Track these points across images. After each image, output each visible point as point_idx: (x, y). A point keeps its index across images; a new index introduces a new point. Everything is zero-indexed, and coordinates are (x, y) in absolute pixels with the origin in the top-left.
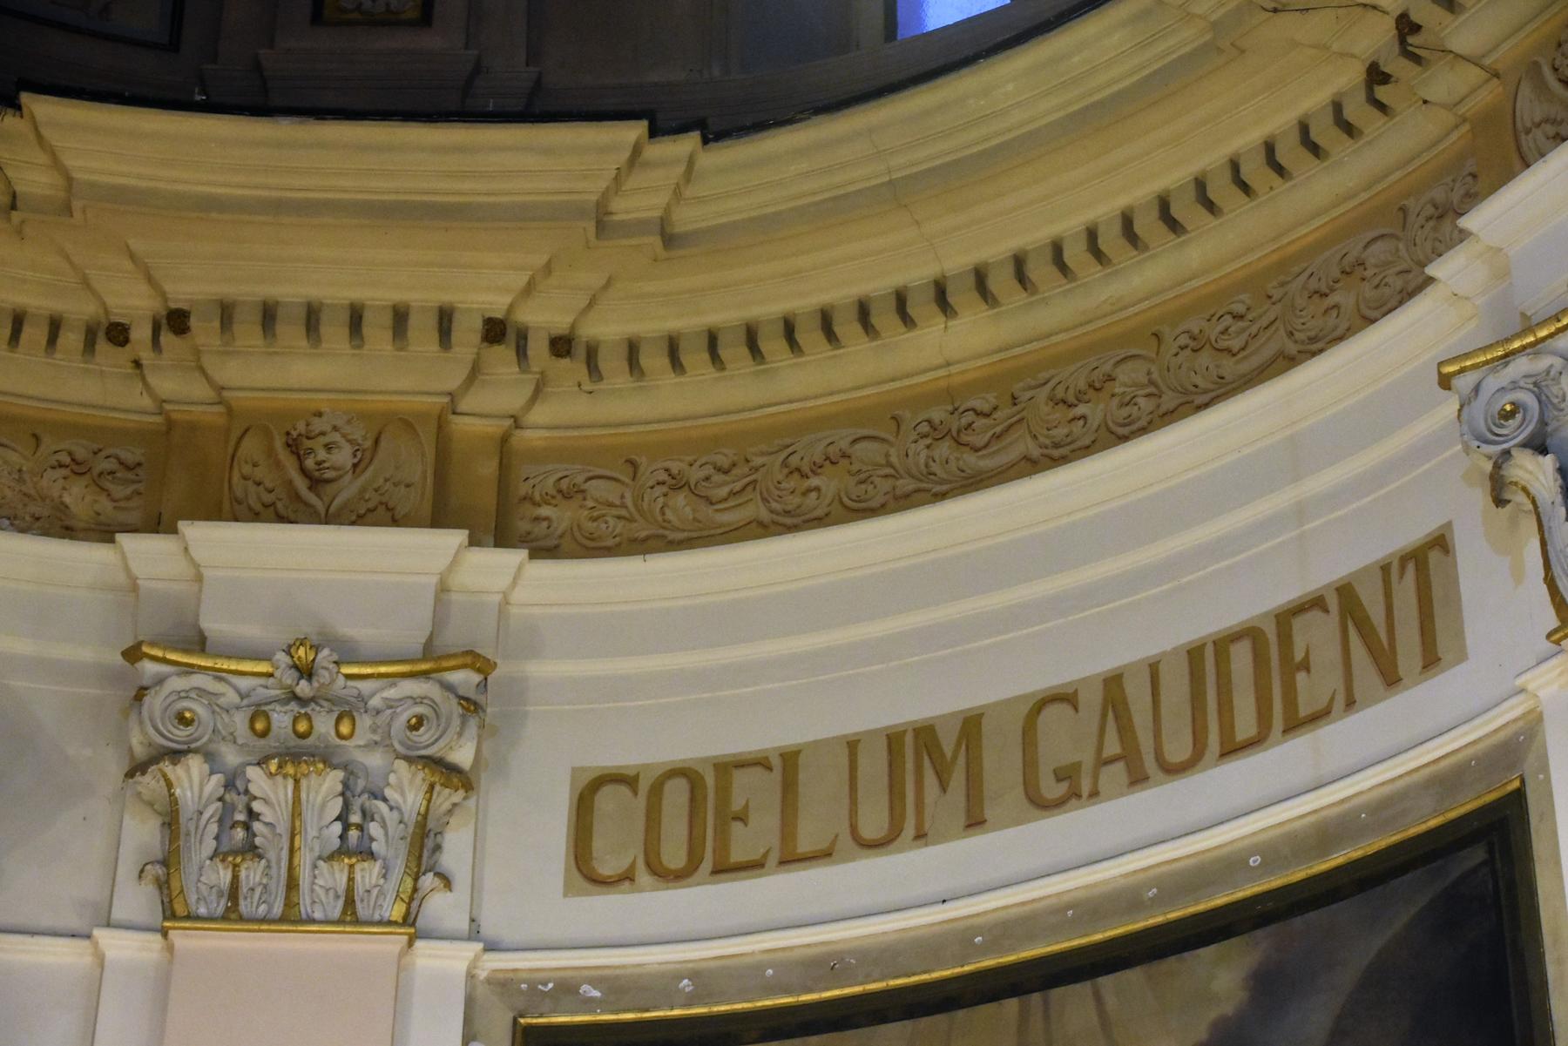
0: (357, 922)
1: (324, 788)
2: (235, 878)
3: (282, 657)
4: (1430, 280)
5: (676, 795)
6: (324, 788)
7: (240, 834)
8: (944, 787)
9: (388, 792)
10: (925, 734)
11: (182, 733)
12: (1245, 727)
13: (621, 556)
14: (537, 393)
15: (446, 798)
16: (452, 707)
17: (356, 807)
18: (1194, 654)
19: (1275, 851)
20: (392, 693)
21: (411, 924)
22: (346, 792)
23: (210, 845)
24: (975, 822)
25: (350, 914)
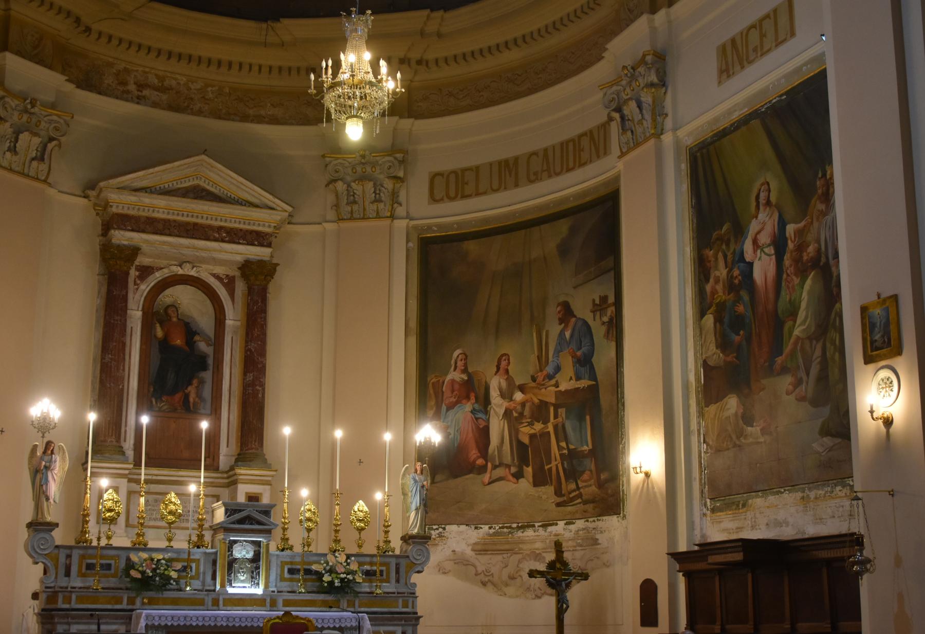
0: (380, 218)
1: (369, 186)
2: (352, 209)
3: (357, 154)
4: (603, 57)
5: (452, 178)
6: (369, 186)
7: (352, 198)
8: (510, 176)
9: (384, 185)
10: (506, 161)
11: (336, 175)
12: (571, 165)
14: (416, 72)
15: (398, 185)
16: (396, 163)
17: (378, 189)
18: (562, 144)
19: (577, 196)
20: (384, 160)
21: (392, 217)
22: (375, 184)
23: (345, 201)
24: (517, 185)
25: (378, 216)
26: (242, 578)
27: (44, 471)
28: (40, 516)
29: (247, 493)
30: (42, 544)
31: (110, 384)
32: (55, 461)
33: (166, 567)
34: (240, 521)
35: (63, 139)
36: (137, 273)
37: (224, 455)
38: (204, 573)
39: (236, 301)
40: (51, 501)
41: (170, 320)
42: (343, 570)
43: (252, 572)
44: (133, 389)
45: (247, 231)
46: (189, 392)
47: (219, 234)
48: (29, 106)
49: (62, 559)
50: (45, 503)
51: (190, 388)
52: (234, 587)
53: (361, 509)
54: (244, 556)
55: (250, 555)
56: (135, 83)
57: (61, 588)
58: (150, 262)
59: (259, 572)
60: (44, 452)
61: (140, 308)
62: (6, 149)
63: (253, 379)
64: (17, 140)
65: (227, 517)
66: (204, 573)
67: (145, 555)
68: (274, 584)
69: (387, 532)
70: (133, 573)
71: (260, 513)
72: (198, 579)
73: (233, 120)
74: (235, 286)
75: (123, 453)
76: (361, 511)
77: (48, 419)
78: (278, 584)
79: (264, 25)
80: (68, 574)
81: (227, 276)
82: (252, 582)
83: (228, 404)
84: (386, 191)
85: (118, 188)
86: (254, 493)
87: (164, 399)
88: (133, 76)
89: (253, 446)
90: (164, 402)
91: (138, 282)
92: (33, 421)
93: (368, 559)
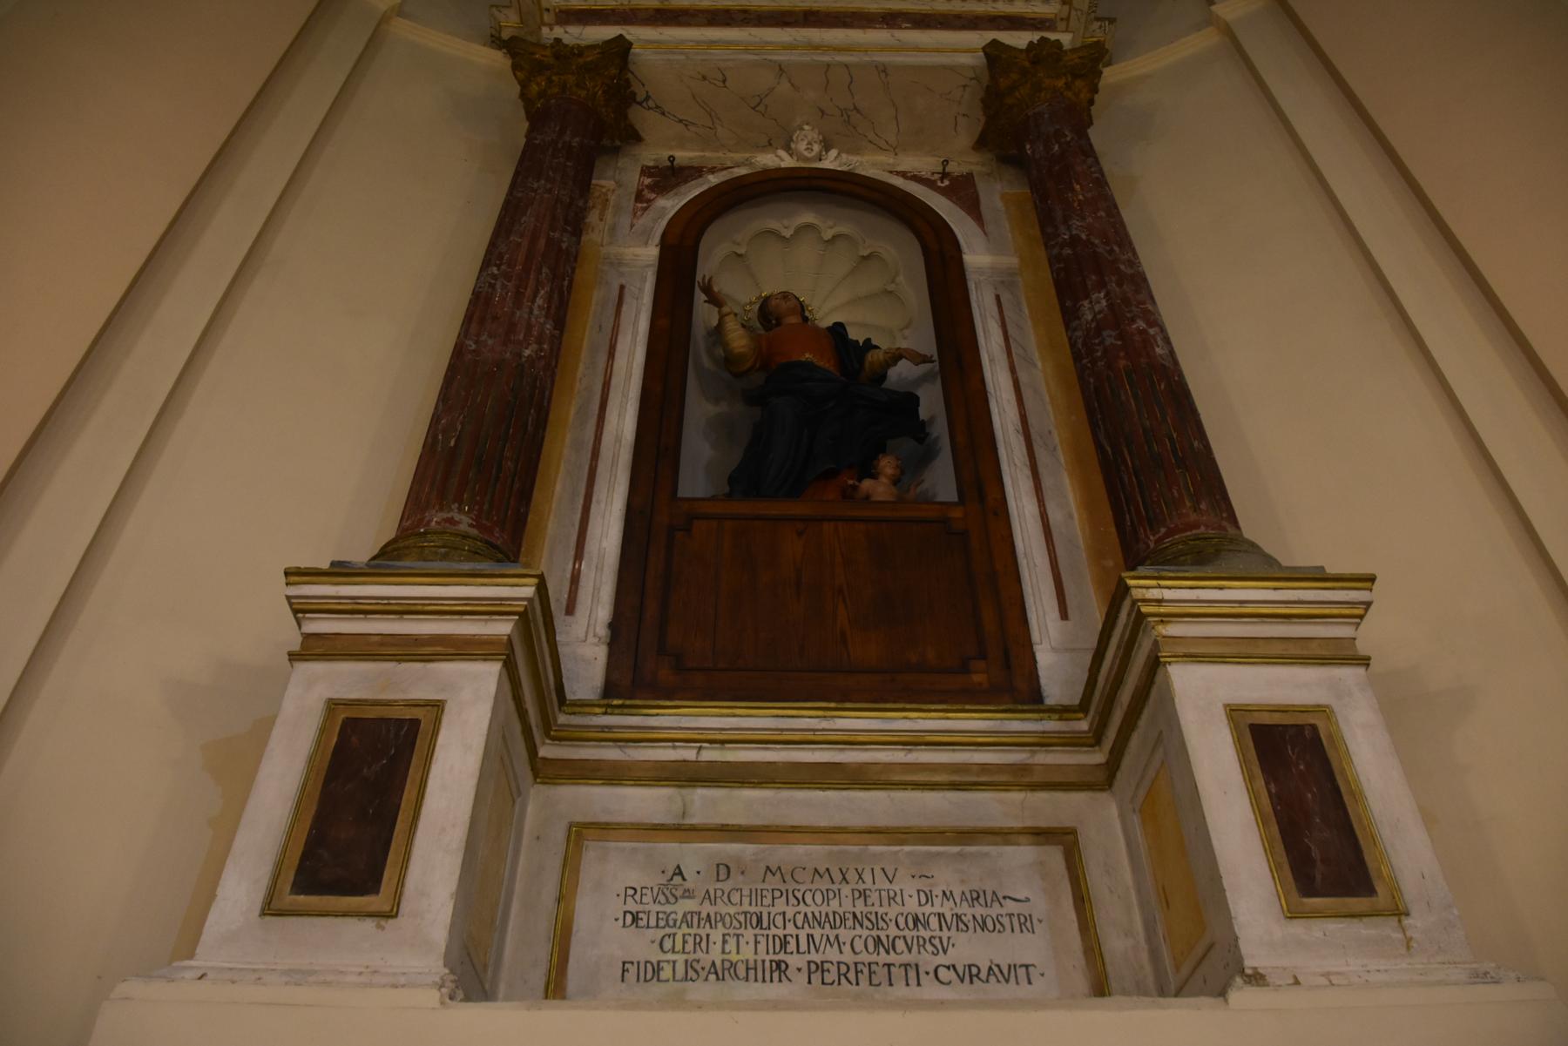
29: (1226, 706)
44: (618, 440)
63: (1111, 306)
83: (1028, 472)
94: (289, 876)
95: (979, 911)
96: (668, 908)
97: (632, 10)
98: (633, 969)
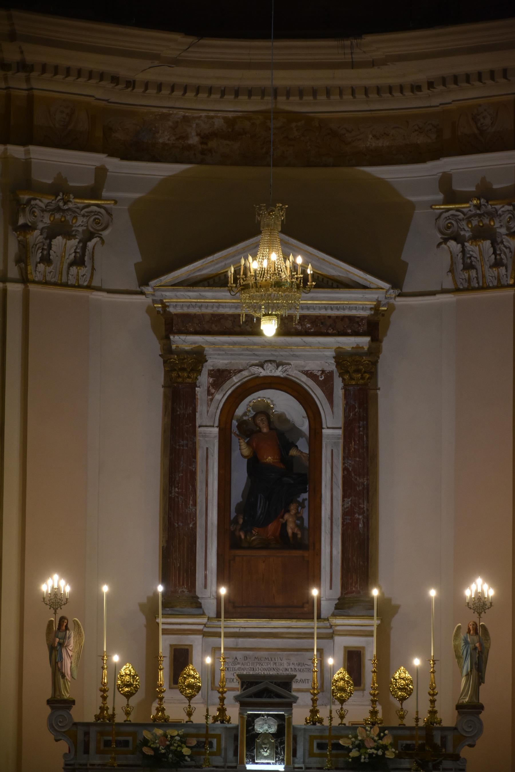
13: (162, 563)
17: (498, 249)
20: (503, 209)
23: (461, 266)
26: (266, 754)
27: (59, 647)
28: (58, 693)
30: (60, 722)
31: (178, 523)
32: (69, 638)
33: (180, 743)
34: (258, 695)
35: (105, 233)
36: (211, 380)
37: (327, 600)
38: (226, 749)
39: (335, 402)
40: (68, 677)
41: (260, 431)
42: (372, 744)
43: (277, 748)
44: (212, 524)
45: (337, 317)
46: (286, 521)
47: (301, 325)
48: (61, 204)
49: (80, 736)
50: (61, 680)
51: (286, 516)
52: (257, 763)
53: (403, 675)
54: (267, 731)
55: (273, 730)
56: (198, 135)
57: (80, 765)
58: (226, 365)
59: (284, 748)
60: (59, 628)
61: (217, 424)
62: (38, 260)
64: (50, 247)
65: (244, 690)
66: (226, 749)
67: (159, 732)
68: (302, 760)
69: (433, 702)
70: (145, 750)
71: (279, 685)
72: (220, 755)
73: (326, 165)
74: (333, 384)
75: (199, 606)
76: (403, 679)
77: (59, 595)
78: (307, 760)
79: (347, 43)
80: (86, 751)
81: (323, 371)
82: (276, 758)
83: (329, 536)
84: (507, 251)
85: (172, 286)
86: (355, 647)
87: (254, 532)
88: (194, 126)
89: (354, 589)
90: (254, 535)
91: (213, 391)
92: (44, 598)
93: (408, 733)
94: (172, 681)
95: (300, 667)
96: (234, 667)
97: (202, 314)
98: (228, 680)
